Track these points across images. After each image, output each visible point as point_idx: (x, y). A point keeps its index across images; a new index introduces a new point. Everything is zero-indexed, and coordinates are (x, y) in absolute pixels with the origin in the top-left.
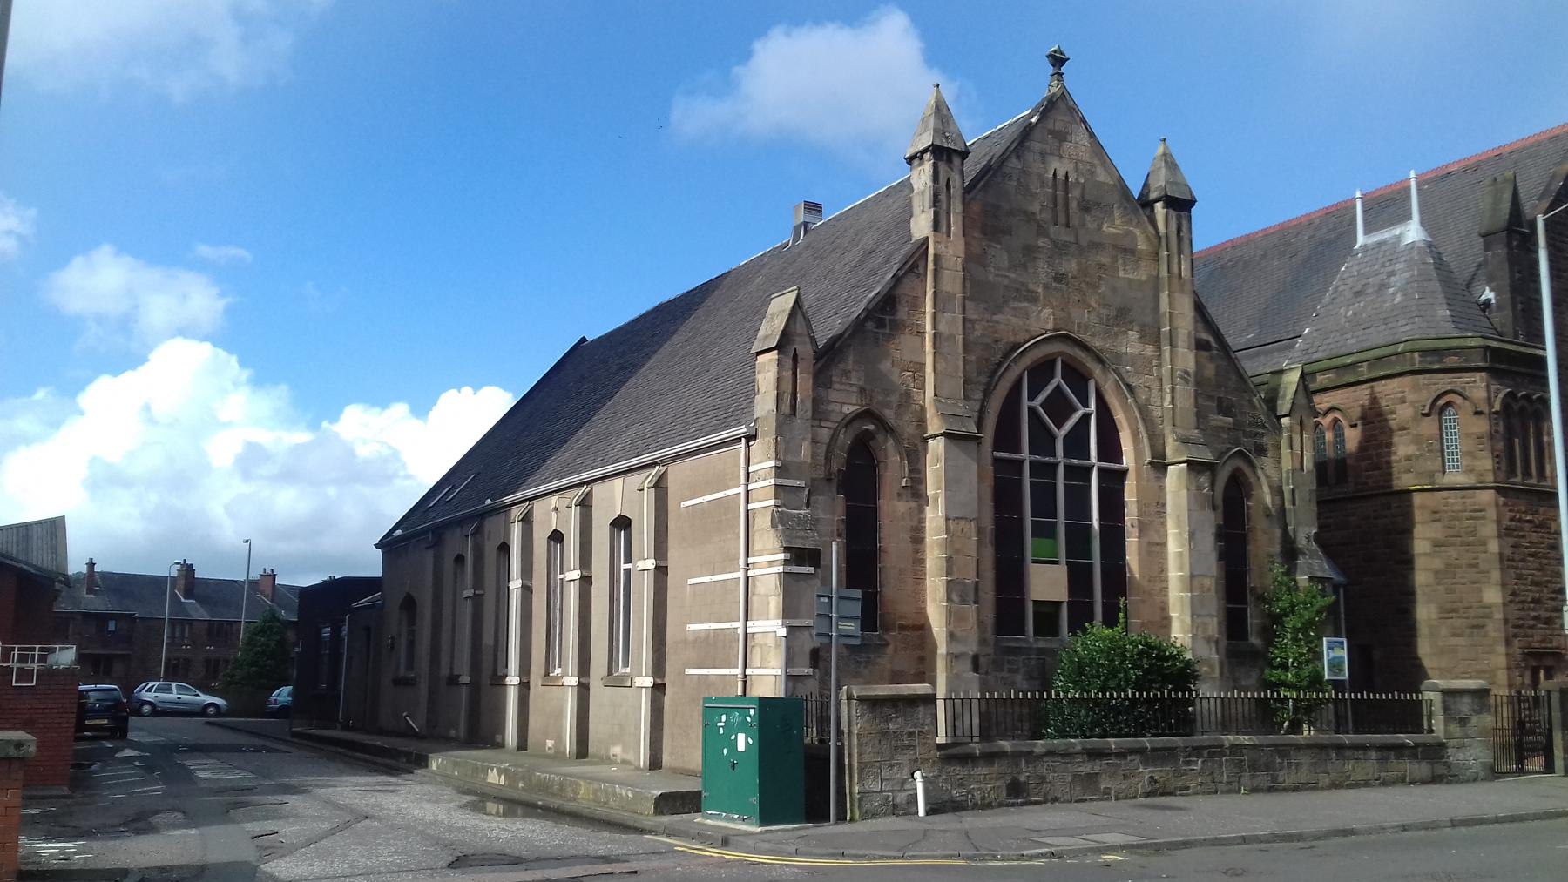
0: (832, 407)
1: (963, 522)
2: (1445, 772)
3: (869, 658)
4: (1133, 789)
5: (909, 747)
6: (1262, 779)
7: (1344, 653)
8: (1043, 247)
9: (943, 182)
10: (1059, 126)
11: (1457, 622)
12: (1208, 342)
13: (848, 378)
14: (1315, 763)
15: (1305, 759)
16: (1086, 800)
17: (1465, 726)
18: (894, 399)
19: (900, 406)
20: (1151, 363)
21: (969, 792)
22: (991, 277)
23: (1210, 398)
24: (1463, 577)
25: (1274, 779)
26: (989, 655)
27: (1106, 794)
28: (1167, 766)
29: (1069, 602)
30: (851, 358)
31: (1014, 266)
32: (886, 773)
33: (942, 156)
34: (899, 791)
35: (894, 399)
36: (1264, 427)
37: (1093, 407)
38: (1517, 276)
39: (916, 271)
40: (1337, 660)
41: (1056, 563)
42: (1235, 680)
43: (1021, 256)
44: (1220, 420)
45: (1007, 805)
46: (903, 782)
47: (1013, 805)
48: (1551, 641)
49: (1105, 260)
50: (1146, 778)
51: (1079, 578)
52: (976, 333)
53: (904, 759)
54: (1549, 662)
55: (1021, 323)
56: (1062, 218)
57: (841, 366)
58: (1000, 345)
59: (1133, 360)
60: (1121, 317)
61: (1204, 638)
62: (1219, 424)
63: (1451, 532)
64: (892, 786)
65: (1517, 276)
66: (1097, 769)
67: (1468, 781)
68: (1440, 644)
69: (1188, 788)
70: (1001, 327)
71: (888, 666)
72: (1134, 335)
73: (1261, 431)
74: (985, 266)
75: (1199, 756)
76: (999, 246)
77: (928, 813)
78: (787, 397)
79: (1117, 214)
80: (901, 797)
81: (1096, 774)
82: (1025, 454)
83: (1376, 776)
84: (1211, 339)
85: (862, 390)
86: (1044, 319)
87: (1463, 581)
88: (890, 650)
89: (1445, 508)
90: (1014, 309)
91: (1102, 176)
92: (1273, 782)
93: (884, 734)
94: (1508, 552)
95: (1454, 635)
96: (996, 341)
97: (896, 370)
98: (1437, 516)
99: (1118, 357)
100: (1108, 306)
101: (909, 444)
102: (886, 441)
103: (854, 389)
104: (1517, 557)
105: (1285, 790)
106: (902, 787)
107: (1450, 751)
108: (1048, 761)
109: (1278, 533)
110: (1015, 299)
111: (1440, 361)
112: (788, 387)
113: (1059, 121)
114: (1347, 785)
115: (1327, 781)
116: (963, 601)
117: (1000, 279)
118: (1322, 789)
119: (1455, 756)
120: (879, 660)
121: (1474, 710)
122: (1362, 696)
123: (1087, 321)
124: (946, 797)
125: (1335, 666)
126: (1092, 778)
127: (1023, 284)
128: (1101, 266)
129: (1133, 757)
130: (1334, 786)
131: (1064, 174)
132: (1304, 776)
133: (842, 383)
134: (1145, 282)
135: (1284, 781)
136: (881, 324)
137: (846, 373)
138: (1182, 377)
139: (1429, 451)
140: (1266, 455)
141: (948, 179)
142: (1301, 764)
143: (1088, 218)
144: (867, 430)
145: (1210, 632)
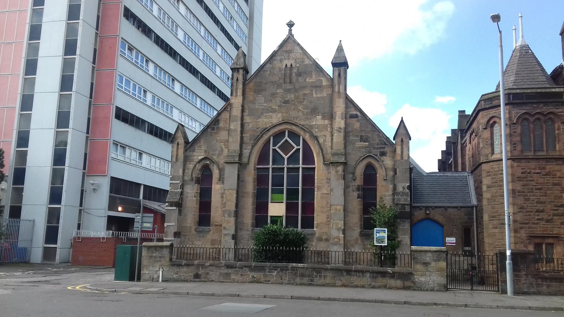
0: (194, 157)
1: (230, 191)
2: (413, 285)
3: (204, 235)
4: (245, 279)
5: (159, 261)
6: (306, 280)
7: (385, 235)
8: (279, 93)
9: (235, 79)
10: (289, 48)
11: (495, 222)
13: (201, 148)
14: (335, 276)
15: (329, 274)
16: (224, 282)
17: (427, 266)
18: (217, 152)
19: (219, 154)
20: (327, 126)
21: (180, 276)
22: (257, 107)
23: (357, 136)
24: (498, 201)
25: (312, 280)
26: (250, 234)
27: (234, 281)
28: (260, 273)
29: (287, 217)
30: (202, 141)
31: (266, 102)
32: (151, 268)
33: (236, 71)
34: (155, 274)
35: (217, 152)
36: (385, 144)
37: (301, 147)
39: (227, 110)
40: (381, 237)
41: (283, 202)
42: (364, 245)
43: (270, 97)
44: (361, 144)
45: (193, 281)
46: (157, 271)
47: (196, 281)
48: (553, 231)
50: (250, 276)
51: (291, 208)
52: (250, 127)
53: (158, 265)
54: (550, 241)
55: (269, 120)
57: (199, 144)
59: (318, 127)
60: (314, 111)
61: (336, 229)
62: (361, 146)
63: (494, 180)
64: (153, 272)
66: (230, 271)
67: (427, 290)
68: (489, 232)
69: (270, 281)
70: (260, 123)
71: (211, 238)
72: (319, 117)
73: (384, 146)
75: (276, 270)
76: (260, 96)
77: (163, 281)
78: (175, 156)
79: (313, 74)
80: (155, 276)
81: (230, 273)
82: (270, 166)
83: (369, 284)
85: (205, 151)
86: (276, 118)
87: (498, 203)
88: (211, 233)
89: (492, 170)
91: (307, 62)
92: (311, 282)
93: (151, 257)
94: (519, 188)
95: (494, 228)
96: (258, 128)
97: (218, 143)
98: (489, 174)
99: (312, 127)
100: (306, 108)
101: (221, 166)
103: (203, 151)
104: (526, 191)
105: (317, 285)
106: (156, 273)
107: (415, 277)
108: (211, 268)
109: (391, 186)
110: (266, 112)
111: (491, 103)
112: (175, 153)
113: (288, 47)
114: (351, 286)
116: (229, 216)
117: (260, 107)
118: (337, 286)
119: (419, 279)
120: (207, 236)
124: (171, 277)
125: (381, 240)
126: (228, 275)
127: (270, 107)
129: (246, 269)
130: (344, 286)
131: (290, 64)
132: (328, 280)
133: (198, 150)
134: (326, 96)
135: (317, 282)
136: (213, 129)
137: (200, 146)
138: (337, 130)
139: (486, 145)
140: (386, 156)
141: (238, 78)
143: (300, 78)
144: (207, 163)
145: (340, 226)
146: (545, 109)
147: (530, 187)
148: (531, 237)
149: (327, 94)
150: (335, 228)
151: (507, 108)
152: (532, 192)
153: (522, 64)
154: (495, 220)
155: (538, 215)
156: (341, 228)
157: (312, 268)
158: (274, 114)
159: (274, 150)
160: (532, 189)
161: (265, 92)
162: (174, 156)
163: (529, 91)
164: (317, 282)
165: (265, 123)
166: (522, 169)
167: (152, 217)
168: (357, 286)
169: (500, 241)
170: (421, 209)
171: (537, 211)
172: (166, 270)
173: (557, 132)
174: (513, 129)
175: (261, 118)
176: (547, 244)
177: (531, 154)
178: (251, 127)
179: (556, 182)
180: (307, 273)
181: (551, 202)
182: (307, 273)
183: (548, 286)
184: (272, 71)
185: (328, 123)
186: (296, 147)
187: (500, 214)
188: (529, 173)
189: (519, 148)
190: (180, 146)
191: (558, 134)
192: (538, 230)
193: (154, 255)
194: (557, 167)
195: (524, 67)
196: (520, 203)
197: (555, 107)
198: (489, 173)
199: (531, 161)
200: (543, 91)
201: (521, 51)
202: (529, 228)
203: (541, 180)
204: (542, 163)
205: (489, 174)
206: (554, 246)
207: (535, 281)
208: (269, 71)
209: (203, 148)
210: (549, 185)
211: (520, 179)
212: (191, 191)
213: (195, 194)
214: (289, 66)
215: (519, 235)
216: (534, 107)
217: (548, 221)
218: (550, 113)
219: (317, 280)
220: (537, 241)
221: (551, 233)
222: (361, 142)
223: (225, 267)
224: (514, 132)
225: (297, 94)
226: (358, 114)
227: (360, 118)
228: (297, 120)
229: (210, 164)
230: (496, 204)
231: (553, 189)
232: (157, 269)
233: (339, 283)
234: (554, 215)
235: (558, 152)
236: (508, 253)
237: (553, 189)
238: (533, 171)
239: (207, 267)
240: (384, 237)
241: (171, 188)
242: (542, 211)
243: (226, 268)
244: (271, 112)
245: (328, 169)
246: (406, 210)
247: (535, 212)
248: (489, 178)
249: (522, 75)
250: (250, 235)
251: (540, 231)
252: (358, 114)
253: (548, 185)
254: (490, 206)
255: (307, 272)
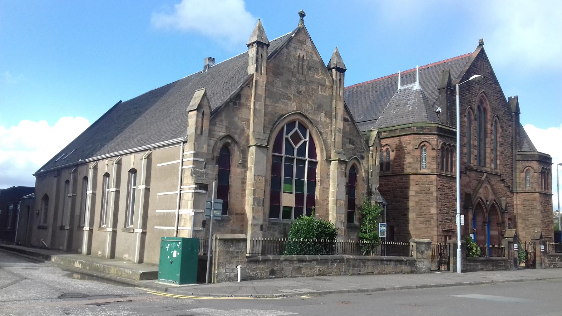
0: (215, 133)
1: (260, 177)
2: (415, 270)
3: (224, 224)
4: (313, 273)
5: (236, 257)
6: (356, 270)
8: (294, 81)
9: (260, 54)
10: (301, 39)
11: (422, 219)
12: (348, 119)
13: (222, 123)
14: (374, 266)
15: (370, 264)
16: (296, 277)
18: (238, 131)
19: (240, 134)
20: (328, 125)
21: (256, 273)
22: (275, 90)
23: (347, 138)
24: (424, 204)
25: (360, 271)
26: (267, 225)
27: (303, 275)
28: (324, 265)
31: (283, 87)
32: (227, 266)
33: (260, 45)
34: (231, 272)
35: (238, 131)
36: (364, 150)
38: (449, 104)
39: (249, 86)
40: (383, 231)
41: (292, 193)
42: (349, 236)
43: (286, 83)
44: (350, 146)
45: (269, 278)
46: (233, 269)
47: (271, 278)
48: (451, 227)
49: (315, 87)
50: (318, 269)
51: (299, 199)
52: (269, 110)
53: (234, 261)
55: (285, 107)
56: (301, 72)
57: (220, 118)
58: (277, 115)
60: (320, 108)
61: (340, 221)
62: (350, 148)
63: (422, 188)
64: (229, 271)
65: (449, 104)
66: (301, 266)
67: (422, 273)
68: (416, 226)
69: (331, 273)
71: (230, 228)
72: (323, 114)
73: (363, 151)
74: (273, 86)
75: (336, 262)
76: (278, 79)
77: (243, 280)
78: (199, 128)
80: (232, 275)
81: (301, 267)
82: (283, 154)
83: (393, 270)
84: (349, 118)
85: (227, 128)
86: (292, 107)
87: (424, 205)
88: (231, 222)
89: (420, 181)
90: (283, 102)
91: (315, 58)
92: (359, 272)
93: (228, 252)
94: (439, 196)
95: (421, 224)
96: (276, 113)
97: (240, 121)
98: (418, 183)
99: (317, 122)
100: (315, 103)
101: (242, 148)
102: (234, 146)
103: (224, 127)
104: (442, 198)
105: (363, 274)
106: (233, 271)
107: (417, 263)
108: (285, 263)
109: (366, 186)
110: (283, 98)
111: (422, 131)
112: (200, 125)
113: (302, 37)
114: (384, 273)
115: (377, 271)
116: (259, 205)
117: (278, 91)
118: (375, 274)
119: (419, 264)
120: (227, 225)
121: (426, 249)
122: (390, 243)
123: (308, 108)
124: (248, 275)
125: (382, 233)
126: (299, 269)
127: (286, 93)
128: (313, 89)
129: (314, 262)
130: (379, 273)
131: (303, 56)
132: (370, 270)
133: (220, 125)
134: (328, 96)
135: (363, 272)
136: (235, 104)
137: (221, 121)
138: (338, 131)
139: (417, 161)
141: (262, 54)
142: (369, 266)
143: (310, 72)
144: (228, 142)
145: (342, 220)
149: (329, 94)
150: (339, 220)
151: (435, 137)
154: (422, 218)
156: (343, 221)
157: (360, 259)
158: (289, 102)
159: (287, 139)
161: (282, 76)
162: (199, 127)
164: (363, 272)
165: (282, 110)
167: (221, 203)
168: (386, 273)
169: (425, 234)
172: (244, 267)
175: (279, 103)
178: (270, 110)
180: (356, 264)
182: (356, 264)
184: (288, 57)
185: (329, 122)
187: (426, 214)
190: (205, 117)
193: (231, 249)
198: (418, 183)
205: (418, 183)
206: (452, 237)
208: (285, 56)
209: (224, 124)
212: (212, 173)
213: (215, 176)
214: (301, 56)
219: (364, 270)
222: (350, 144)
223: (297, 261)
225: (308, 87)
226: (349, 120)
227: (350, 122)
228: (307, 112)
229: (231, 143)
230: (423, 206)
232: (234, 266)
233: (377, 271)
235: (454, 173)
239: (282, 261)
240: (385, 230)
241: (194, 166)
243: (298, 263)
244: (287, 99)
245: (328, 165)
246: (247, 196)
248: (418, 186)
250: (268, 226)
252: (349, 120)
254: (417, 207)
255: (357, 263)
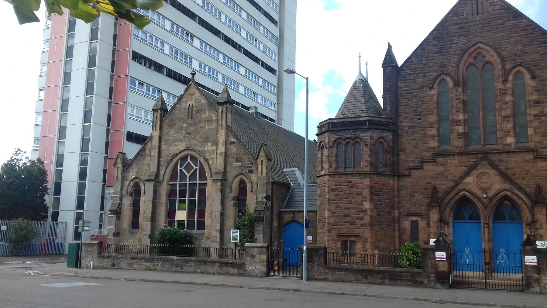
1: (148, 202)
2: (244, 272)
5: (92, 254)
6: (178, 268)
7: (238, 235)
9: (155, 117)
10: (191, 92)
12: (234, 142)
15: (193, 264)
17: (254, 258)
18: (143, 173)
23: (234, 158)
25: (182, 269)
29: (188, 221)
30: (134, 165)
31: (176, 134)
35: (143, 173)
37: (198, 168)
38: (388, 84)
41: (185, 210)
47: (112, 269)
49: (202, 125)
51: (190, 214)
53: (91, 257)
54: (353, 239)
56: (190, 117)
57: (132, 167)
58: (171, 155)
59: (209, 152)
60: (206, 140)
62: (236, 165)
65: (388, 84)
67: (253, 276)
69: (156, 269)
70: (171, 150)
71: (138, 237)
72: (210, 144)
74: (168, 135)
77: (93, 268)
79: (207, 110)
83: (217, 271)
84: (235, 140)
85: (136, 172)
86: (181, 146)
88: (139, 233)
90: (176, 144)
94: (333, 197)
97: (144, 166)
99: (205, 151)
102: (141, 183)
103: (135, 172)
107: (246, 266)
108: (122, 259)
109: (255, 196)
115: (199, 271)
116: (147, 221)
119: (249, 268)
121: (258, 254)
122: (177, 245)
123: (196, 143)
124: (98, 265)
125: (235, 238)
127: (178, 137)
128: (201, 127)
130: (202, 273)
132: (192, 269)
136: (142, 155)
137: (133, 169)
138: (220, 154)
140: (252, 173)
142: (192, 266)
143: (198, 115)
145: (217, 228)
146: (354, 135)
147: (341, 196)
148: (340, 236)
152: (342, 200)
153: (352, 97)
155: (345, 219)
159: (181, 170)
160: (342, 198)
163: (343, 120)
166: (335, 182)
168: (209, 273)
170: (289, 214)
171: (344, 216)
173: (361, 152)
174: (331, 151)
176: (351, 242)
177: (341, 170)
179: (359, 192)
181: (354, 208)
183: (332, 274)
186: (195, 168)
188: (340, 185)
189: (334, 166)
191: (362, 154)
192: (345, 231)
193: (89, 249)
194: (360, 181)
195: (353, 99)
196: (333, 209)
197: (361, 133)
199: (342, 176)
200: (353, 120)
201: (355, 85)
202: (338, 229)
203: (348, 191)
204: (350, 177)
207: (324, 270)
210: (353, 195)
211: (333, 190)
214: (191, 106)
215: (331, 234)
216: (346, 133)
217: (351, 223)
218: (357, 137)
219: (186, 269)
220: (344, 239)
221: (353, 233)
224: (331, 154)
231: (357, 198)
233: (199, 271)
234: (356, 219)
236: (305, 248)
237: (357, 198)
238: (343, 184)
240: (237, 236)
242: (348, 215)
247: (343, 216)
249: (349, 106)
251: (346, 231)
253: (352, 195)
